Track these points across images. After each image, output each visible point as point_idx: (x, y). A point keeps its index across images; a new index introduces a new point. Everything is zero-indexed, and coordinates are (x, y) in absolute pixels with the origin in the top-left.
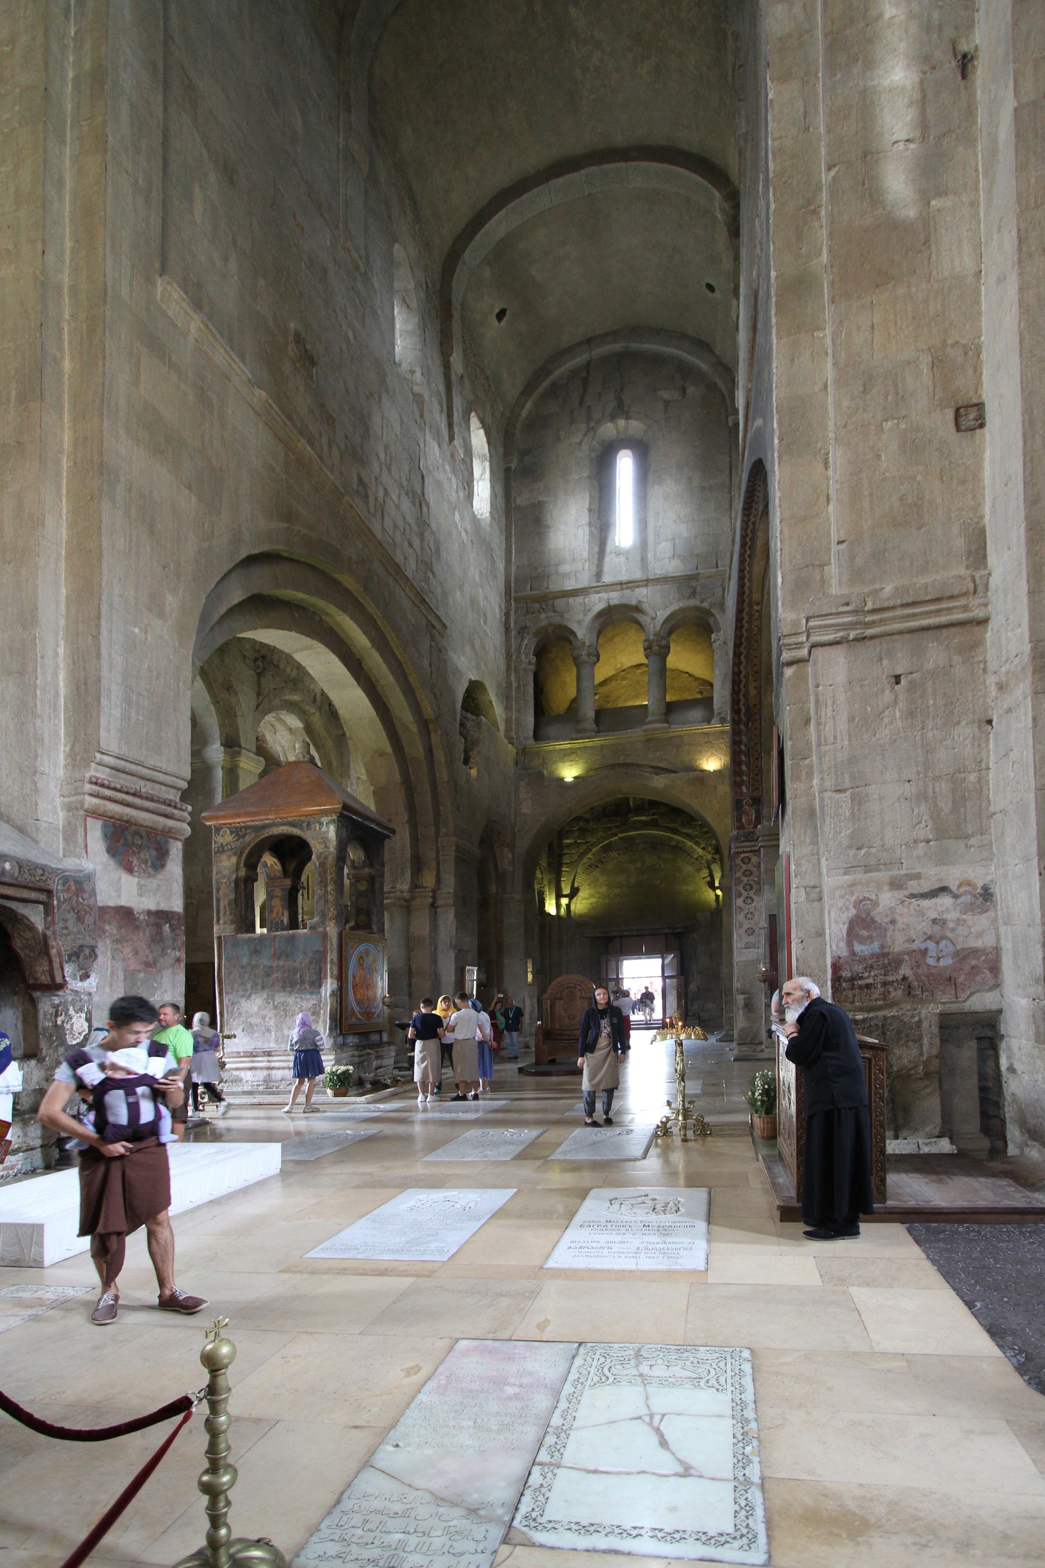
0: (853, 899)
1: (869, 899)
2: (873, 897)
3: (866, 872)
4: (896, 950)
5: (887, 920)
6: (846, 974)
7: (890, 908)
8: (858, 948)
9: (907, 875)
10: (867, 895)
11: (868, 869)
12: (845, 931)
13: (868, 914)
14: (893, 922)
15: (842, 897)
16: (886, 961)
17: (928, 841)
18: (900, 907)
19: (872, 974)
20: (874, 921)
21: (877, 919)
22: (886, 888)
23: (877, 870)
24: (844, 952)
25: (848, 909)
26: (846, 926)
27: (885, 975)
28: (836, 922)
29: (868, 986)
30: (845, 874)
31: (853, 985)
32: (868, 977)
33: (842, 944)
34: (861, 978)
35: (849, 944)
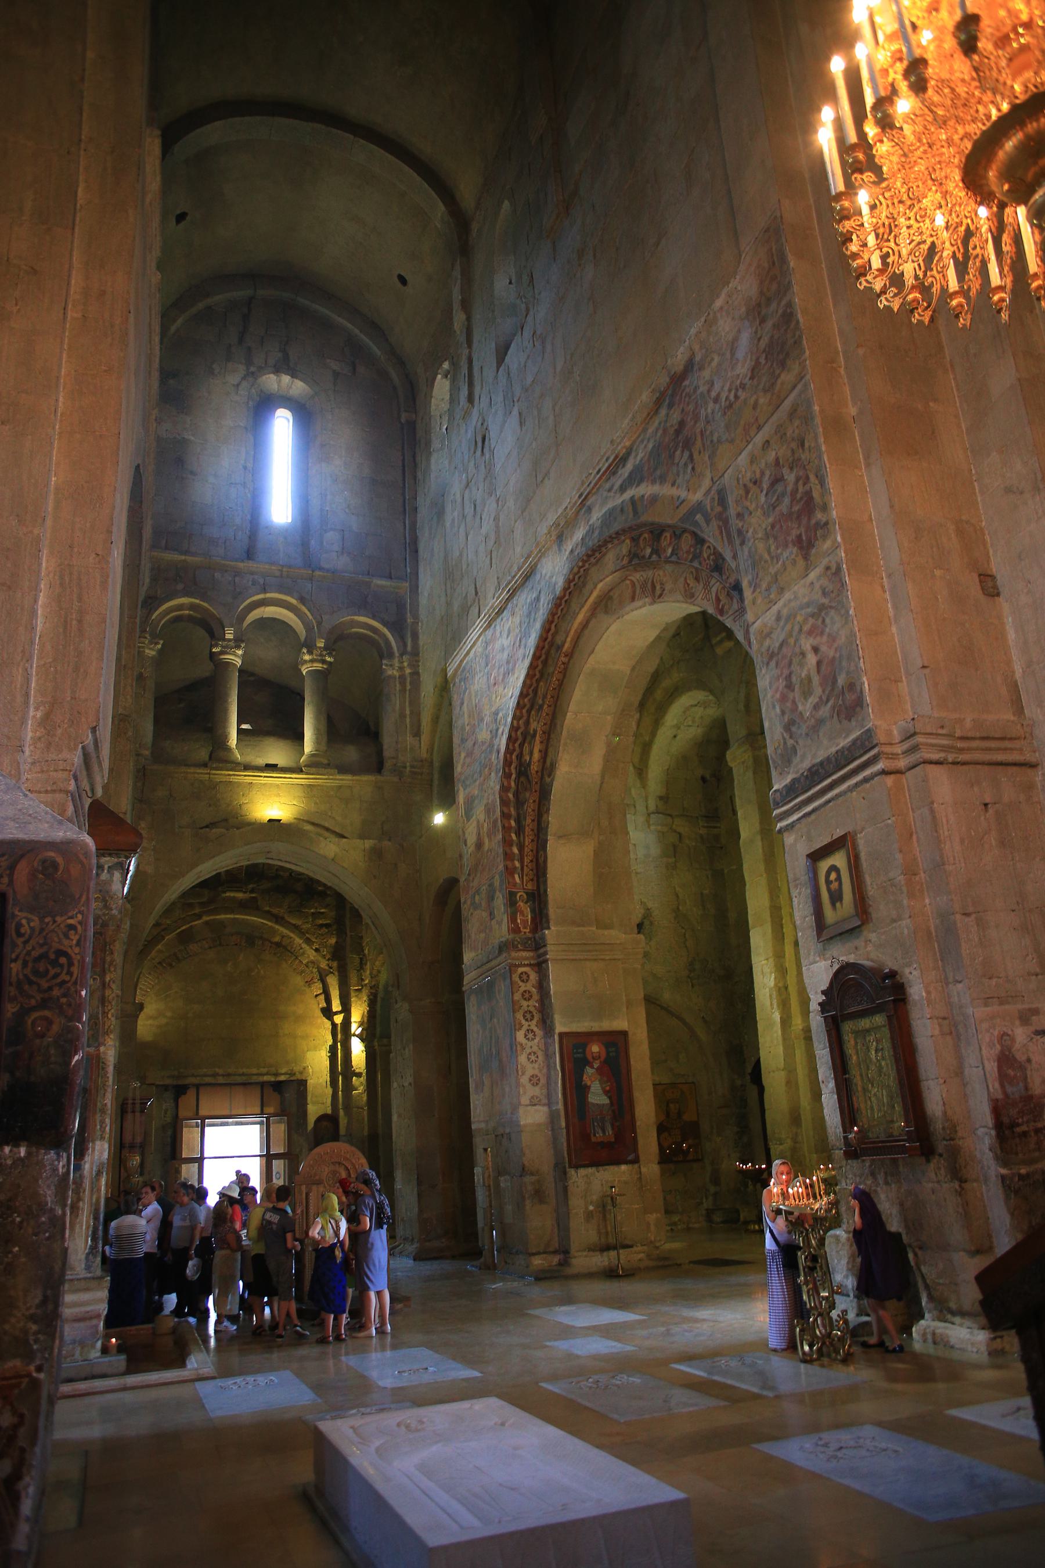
0: (996, 1033)
1: (1008, 1035)
2: (1010, 1033)
3: (1001, 1004)
4: (1037, 1092)
5: (1024, 1058)
6: (1006, 1120)
7: (1024, 1045)
8: (1009, 1089)
9: (1030, 1010)
10: (1005, 1029)
11: (1002, 1001)
12: (996, 1069)
13: (1010, 1051)
14: (1029, 1060)
15: (988, 1031)
16: (1032, 1105)
17: (1037, 975)
18: (1031, 1044)
19: (1025, 1119)
20: (1015, 1059)
21: (1018, 1057)
22: (1017, 1022)
23: (1009, 1003)
24: (1000, 1096)
25: (994, 1045)
26: (996, 1064)
27: (1035, 1121)
28: (988, 1060)
29: (1025, 1134)
30: (986, 1005)
31: (1013, 1132)
32: (1022, 1124)
33: (997, 1085)
34: (1018, 1125)
35: (1002, 1086)
